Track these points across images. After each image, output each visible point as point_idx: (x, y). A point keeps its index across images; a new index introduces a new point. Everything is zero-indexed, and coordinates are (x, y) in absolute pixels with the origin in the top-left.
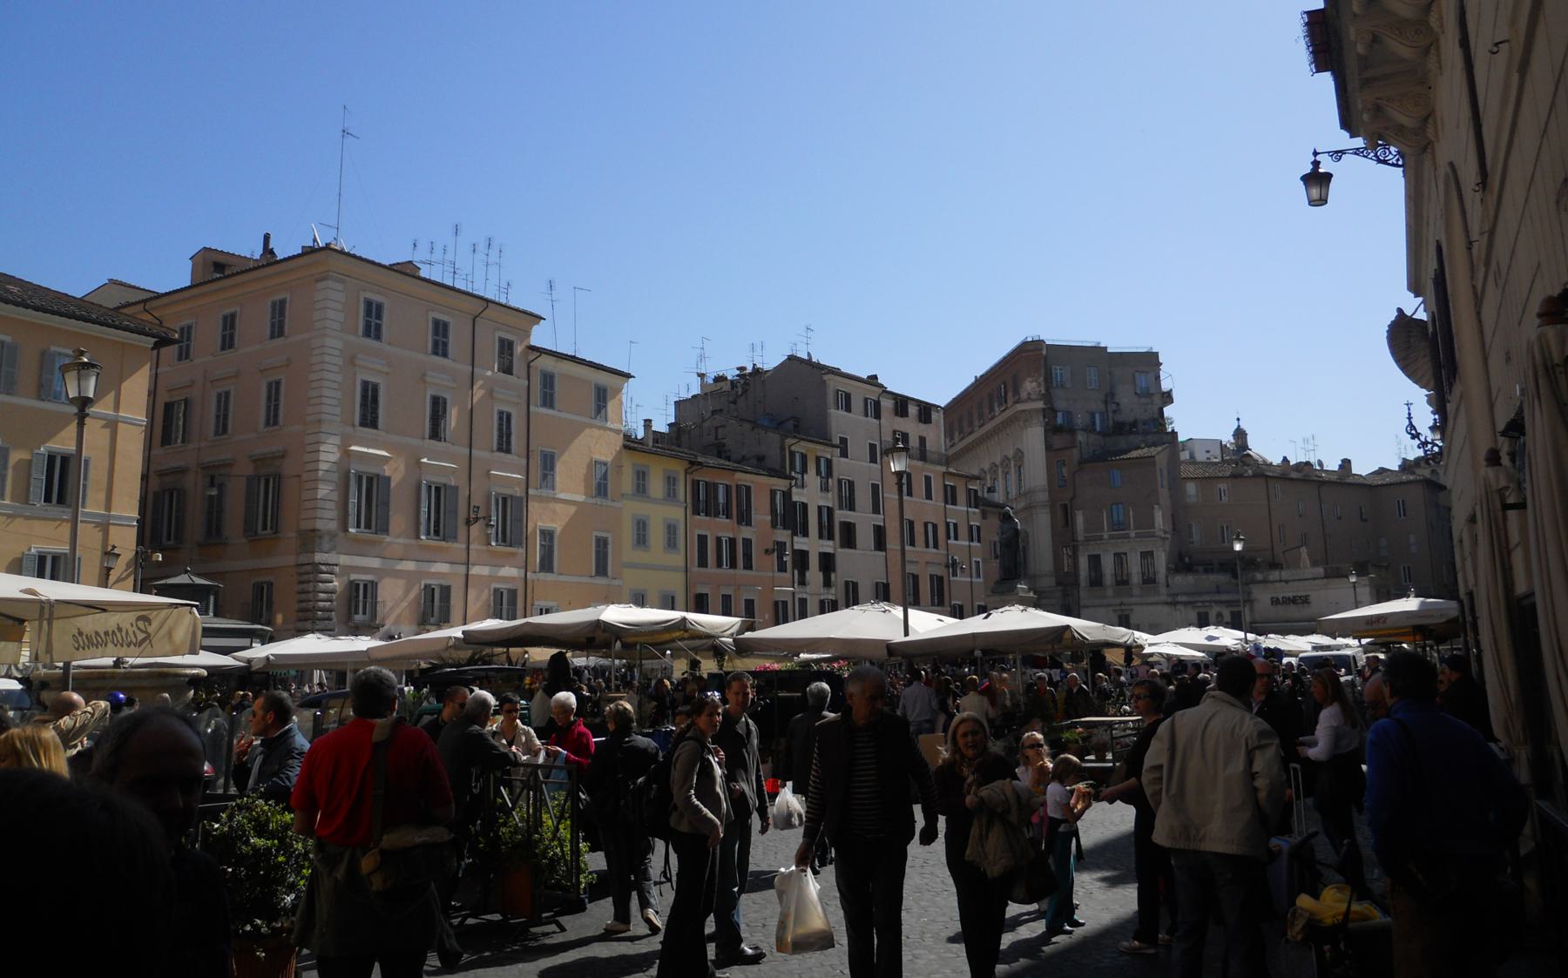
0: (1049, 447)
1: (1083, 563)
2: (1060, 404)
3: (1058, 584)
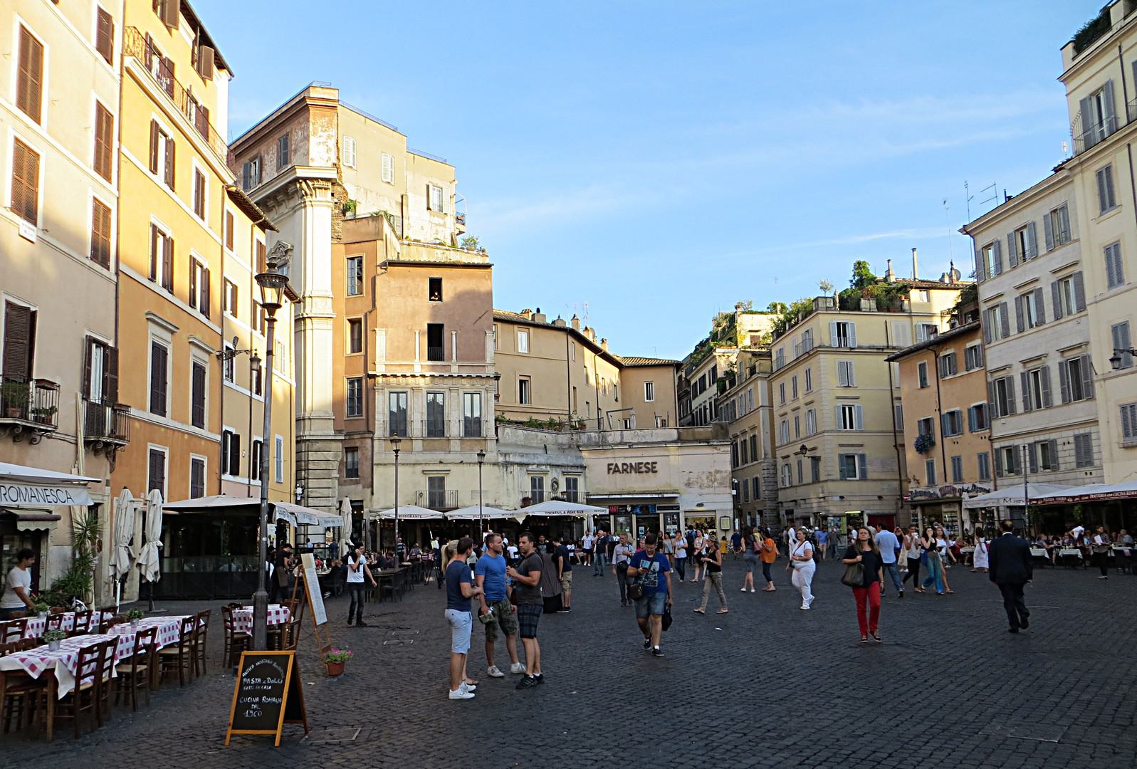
0: (336, 238)
3: (338, 432)
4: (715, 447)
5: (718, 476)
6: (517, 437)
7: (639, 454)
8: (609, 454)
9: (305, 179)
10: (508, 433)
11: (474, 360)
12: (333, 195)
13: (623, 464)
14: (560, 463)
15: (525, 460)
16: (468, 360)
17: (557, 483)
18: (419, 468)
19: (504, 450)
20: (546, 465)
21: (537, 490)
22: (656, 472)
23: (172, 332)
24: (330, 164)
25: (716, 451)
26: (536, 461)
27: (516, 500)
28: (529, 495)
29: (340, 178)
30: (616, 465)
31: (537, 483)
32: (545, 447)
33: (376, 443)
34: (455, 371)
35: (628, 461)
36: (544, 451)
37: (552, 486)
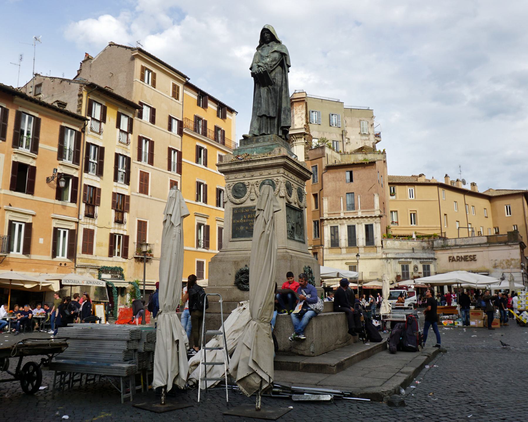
1: (327, 232)
2: (314, 134)
4: (510, 245)
5: (513, 262)
6: (395, 244)
7: (466, 250)
8: (449, 251)
10: (389, 243)
11: (369, 208)
12: (305, 139)
13: (457, 257)
14: (418, 257)
15: (397, 256)
16: (366, 208)
17: (417, 267)
18: (344, 262)
19: (386, 251)
20: (410, 258)
21: (405, 271)
22: (476, 260)
23: (207, 218)
24: (303, 126)
25: (510, 248)
26: (404, 257)
28: (400, 273)
29: (309, 131)
30: (453, 258)
31: (405, 268)
32: (413, 249)
33: (325, 250)
34: (360, 214)
35: (460, 255)
36: (411, 251)
37: (414, 269)
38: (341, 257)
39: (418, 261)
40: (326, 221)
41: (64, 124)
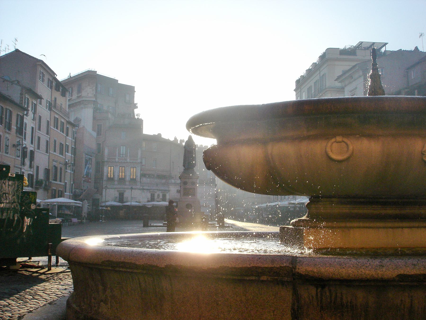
9: (86, 100)
10: (144, 180)
27: (146, 200)
28: (150, 199)
31: (153, 196)
38: (115, 187)
39: (160, 192)
40: (106, 163)
41: (19, 113)
